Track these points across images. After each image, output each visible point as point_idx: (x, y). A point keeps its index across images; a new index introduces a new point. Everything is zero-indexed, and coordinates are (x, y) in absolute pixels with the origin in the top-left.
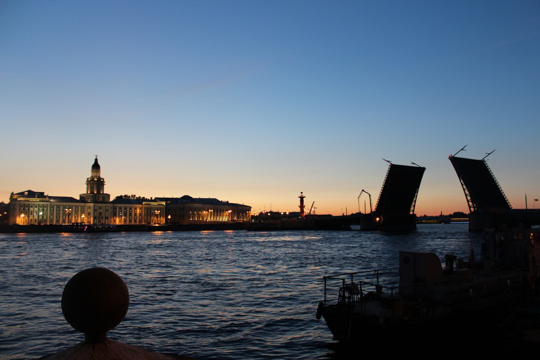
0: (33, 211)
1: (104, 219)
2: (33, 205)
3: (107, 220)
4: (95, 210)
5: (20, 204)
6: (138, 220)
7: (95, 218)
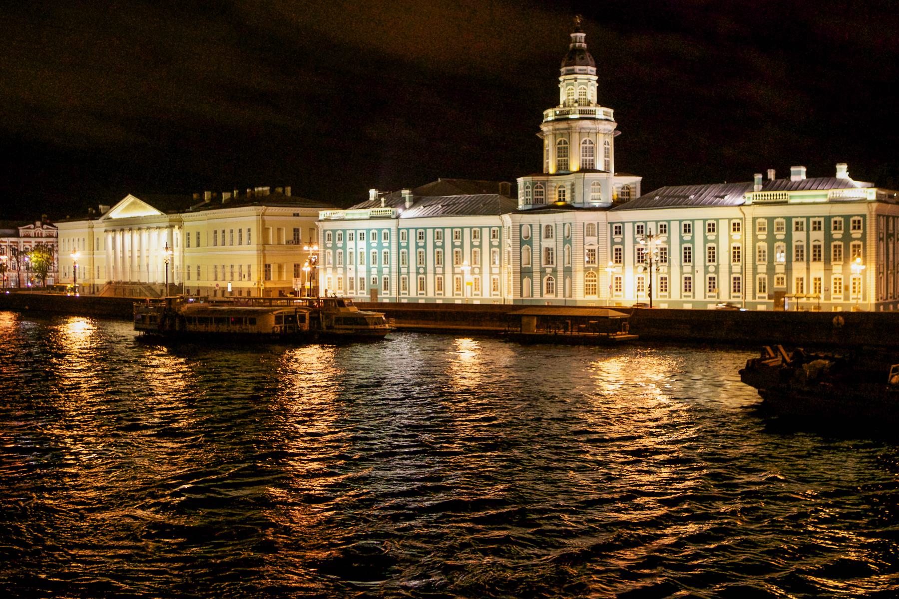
0: (354, 251)
1: (560, 275)
3: (567, 281)
4: (524, 241)
5: (325, 231)
7: (524, 273)
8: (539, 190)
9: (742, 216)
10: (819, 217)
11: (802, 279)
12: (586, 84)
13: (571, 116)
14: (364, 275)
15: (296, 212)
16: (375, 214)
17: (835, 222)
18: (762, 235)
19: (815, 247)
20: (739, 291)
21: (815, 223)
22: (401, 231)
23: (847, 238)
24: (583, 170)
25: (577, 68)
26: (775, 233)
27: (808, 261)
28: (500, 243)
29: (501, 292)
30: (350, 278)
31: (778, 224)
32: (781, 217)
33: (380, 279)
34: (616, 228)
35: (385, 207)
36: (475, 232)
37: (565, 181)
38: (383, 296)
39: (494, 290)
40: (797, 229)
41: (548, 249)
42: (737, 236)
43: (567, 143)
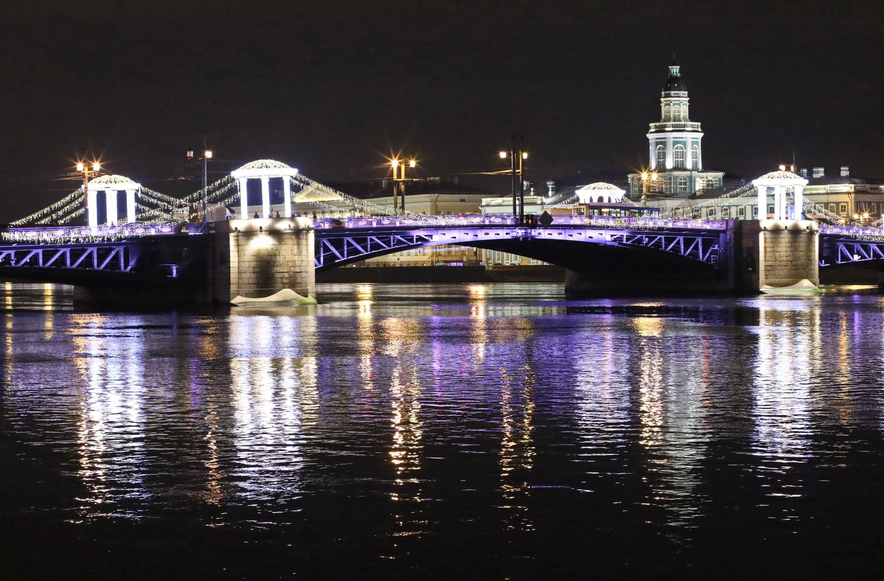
12: (679, 104)
13: (667, 129)
15: (462, 198)
24: (676, 169)
25: (672, 93)
35: (534, 195)
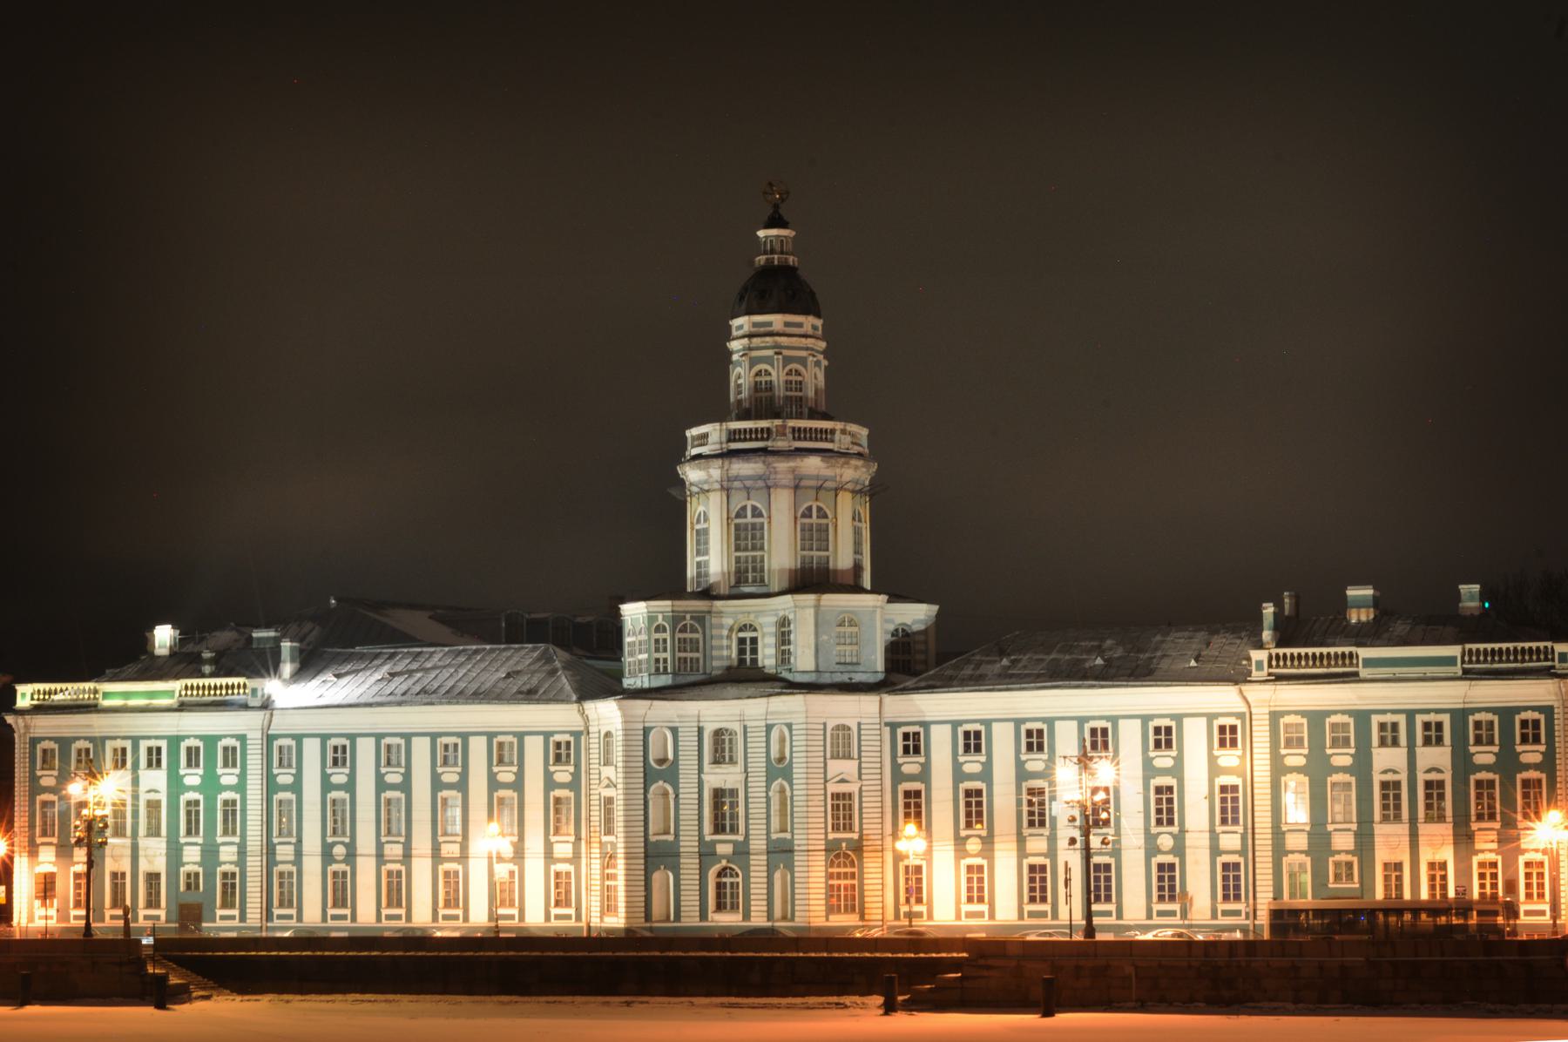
1: (758, 863)
2: (128, 744)
5: (34, 742)
6: (1199, 881)
8: (688, 635)
9: (1244, 709)
10: (1438, 711)
11: (1398, 866)
12: (803, 361)
14: (160, 865)
16: (194, 697)
17: (1478, 725)
18: (1296, 758)
19: (1428, 784)
20: (1237, 898)
21: (1427, 726)
22: (276, 744)
23: (1508, 763)
26: (1329, 751)
27: (1413, 821)
28: (576, 776)
29: (578, 909)
30: (114, 875)
31: (1334, 726)
32: (1343, 712)
33: (210, 875)
34: (906, 736)
36: (501, 745)
37: (759, 613)
38: (219, 923)
39: (557, 904)
40: (1383, 743)
41: (718, 794)
42: (1228, 758)
43: (760, 515)
